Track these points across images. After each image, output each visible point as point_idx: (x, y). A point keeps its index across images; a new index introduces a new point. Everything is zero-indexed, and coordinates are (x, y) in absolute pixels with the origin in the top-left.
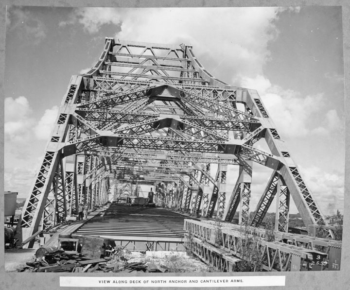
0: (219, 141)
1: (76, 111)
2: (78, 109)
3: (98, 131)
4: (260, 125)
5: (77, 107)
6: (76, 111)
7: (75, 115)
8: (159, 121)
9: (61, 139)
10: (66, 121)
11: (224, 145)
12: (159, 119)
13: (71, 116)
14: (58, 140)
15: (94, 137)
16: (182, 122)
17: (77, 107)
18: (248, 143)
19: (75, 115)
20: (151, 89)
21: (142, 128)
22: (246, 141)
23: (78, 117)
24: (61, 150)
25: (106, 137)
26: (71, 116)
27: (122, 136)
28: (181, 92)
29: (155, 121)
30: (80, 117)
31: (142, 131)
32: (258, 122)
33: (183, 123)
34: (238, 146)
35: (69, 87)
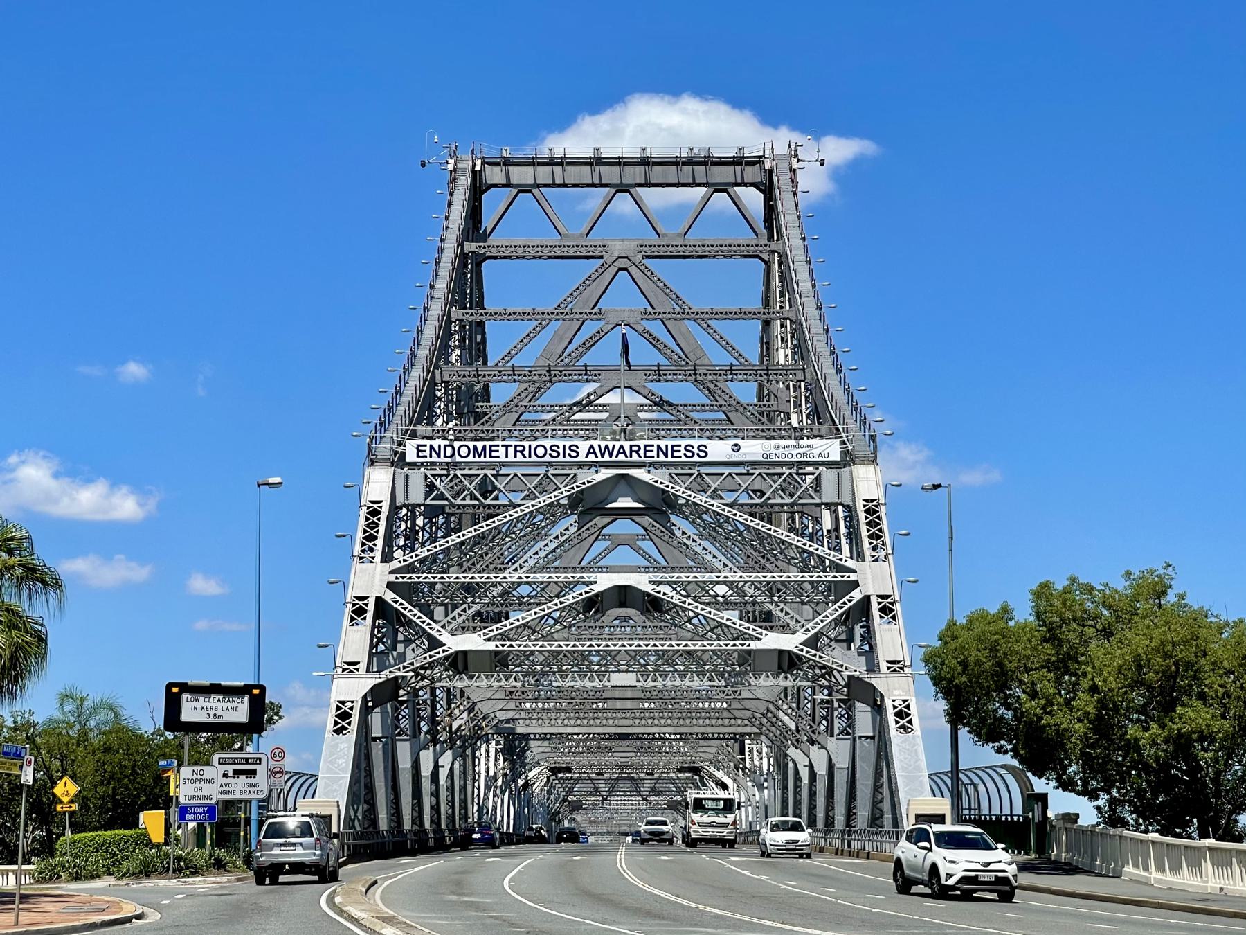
0: (737, 643)
1: (390, 586)
2: (392, 578)
3: (445, 638)
4: (856, 584)
5: (391, 572)
6: (390, 586)
7: (389, 596)
8: (597, 595)
9: (363, 666)
10: (370, 615)
11: (749, 652)
12: (597, 588)
13: (380, 601)
14: (357, 670)
15: (439, 654)
16: (652, 592)
17: (391, 572)
18: (812, 642)
19: (389, 596)
20: (582, 492)
21: (552, 618)
22: (806, 637)
23: (396, 602)
24: (366, 695)
25: (465, 653)
26: (380, 601)
27: (503, 646)
28: (664, 491)
29: (584, 596)
30: (401, 601)
31: (555, 625)
32: (853, 577)
33: (656, 598)
34: (781, 652)
35: (363, 513)
